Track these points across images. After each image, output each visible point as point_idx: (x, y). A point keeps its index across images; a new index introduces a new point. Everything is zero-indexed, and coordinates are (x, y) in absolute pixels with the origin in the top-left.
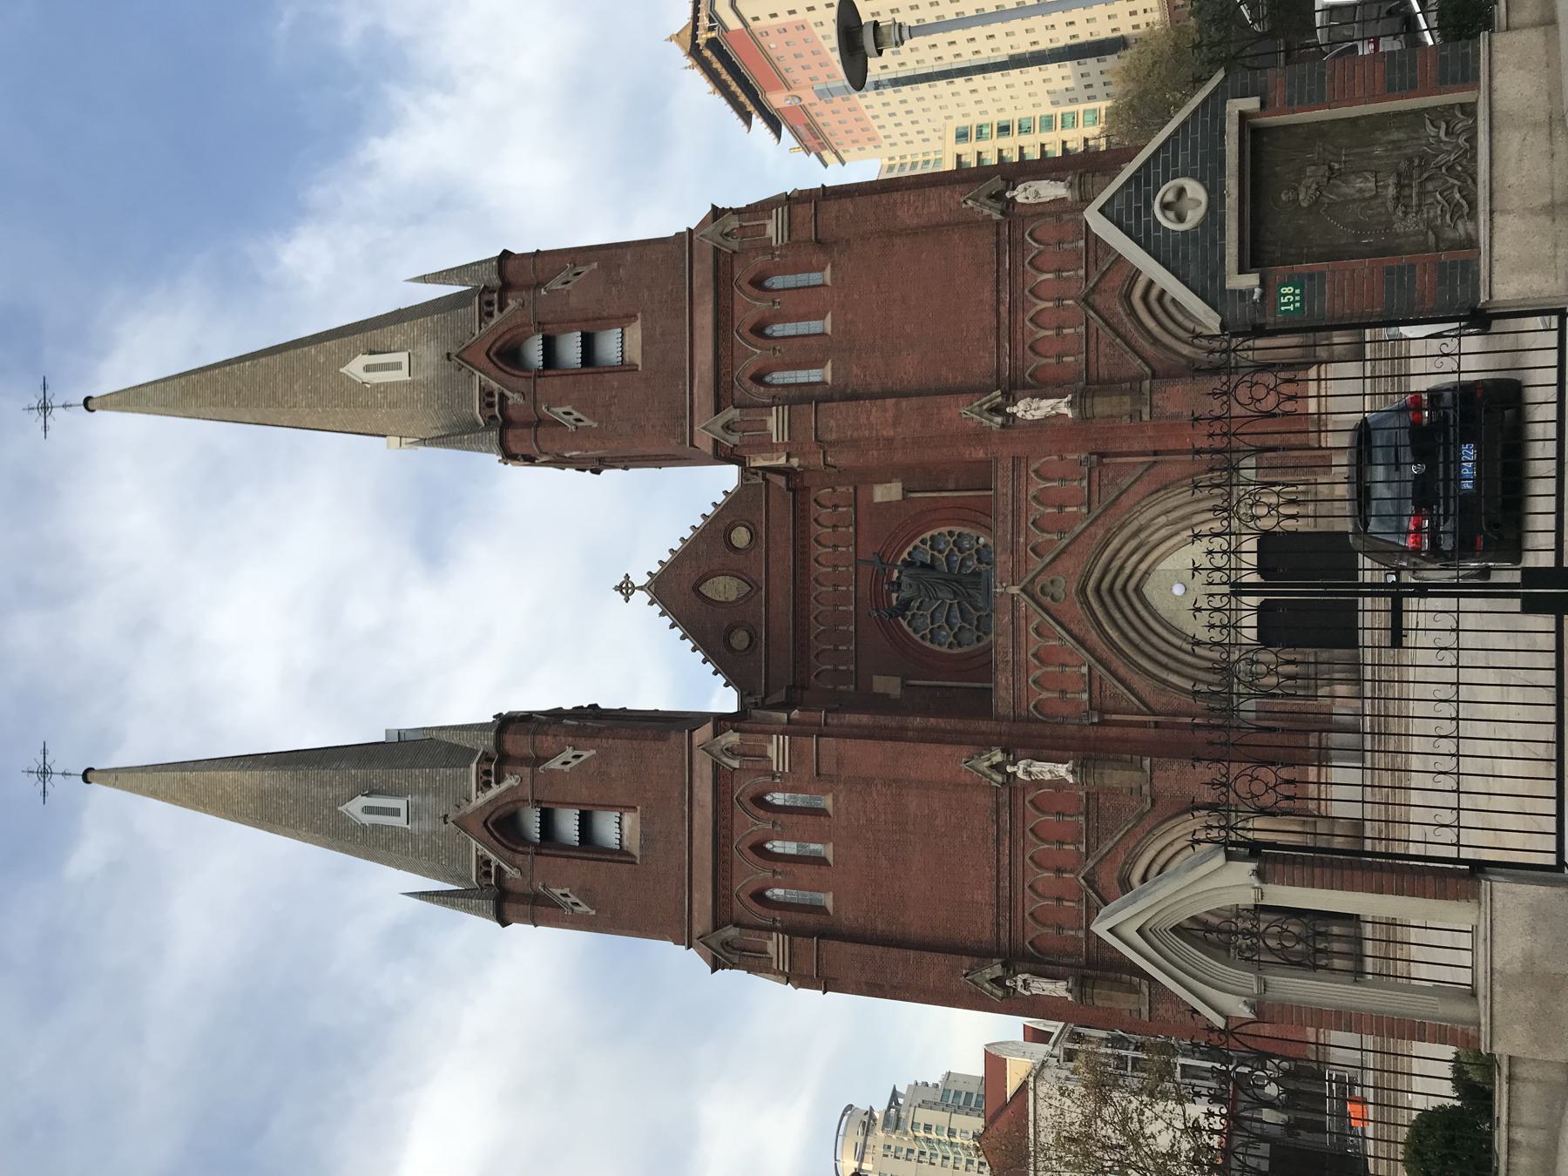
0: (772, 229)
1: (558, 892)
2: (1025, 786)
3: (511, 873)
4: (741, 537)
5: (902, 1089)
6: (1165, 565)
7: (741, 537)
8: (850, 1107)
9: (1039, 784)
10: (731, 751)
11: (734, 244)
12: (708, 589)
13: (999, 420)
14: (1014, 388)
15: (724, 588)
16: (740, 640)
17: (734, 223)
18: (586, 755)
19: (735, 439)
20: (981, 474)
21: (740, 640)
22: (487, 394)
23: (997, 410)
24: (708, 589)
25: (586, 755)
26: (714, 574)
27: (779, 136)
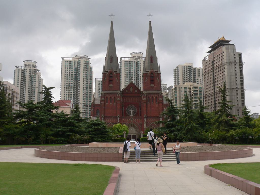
0: (160, 99)
1: (106, 79)
2: (117, 119)
3: (107, 74)
4: (136, 91)
5: (40, 71)
6: (134, 129)
7: (136, 91)
8: (36, 62)
9: (117, 120)
10: (119, 95)
11: (159, 95)
12: (131, 88)
13: (144, 117)
14: (147, 118)
15: (131, 89)
16: (127, 91)
17: (161, 95)
18: (117, 81)
19: (144, 95)
20: (141, 115)
21: (127, 91)
22: (149, 71)
23: (145, 117)
24: (131, 88)
25: (117, 81)
26: (133, 89)
27: (208, 53)
